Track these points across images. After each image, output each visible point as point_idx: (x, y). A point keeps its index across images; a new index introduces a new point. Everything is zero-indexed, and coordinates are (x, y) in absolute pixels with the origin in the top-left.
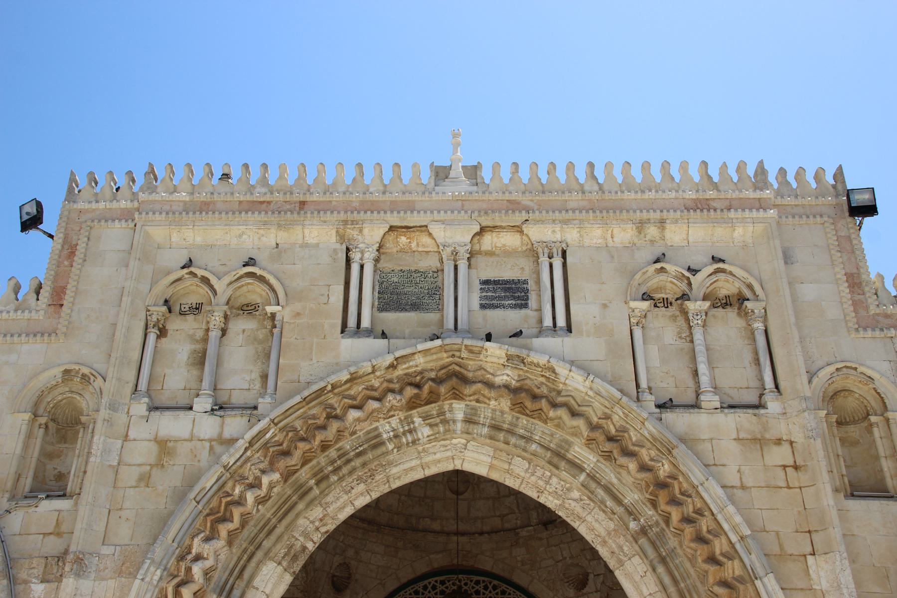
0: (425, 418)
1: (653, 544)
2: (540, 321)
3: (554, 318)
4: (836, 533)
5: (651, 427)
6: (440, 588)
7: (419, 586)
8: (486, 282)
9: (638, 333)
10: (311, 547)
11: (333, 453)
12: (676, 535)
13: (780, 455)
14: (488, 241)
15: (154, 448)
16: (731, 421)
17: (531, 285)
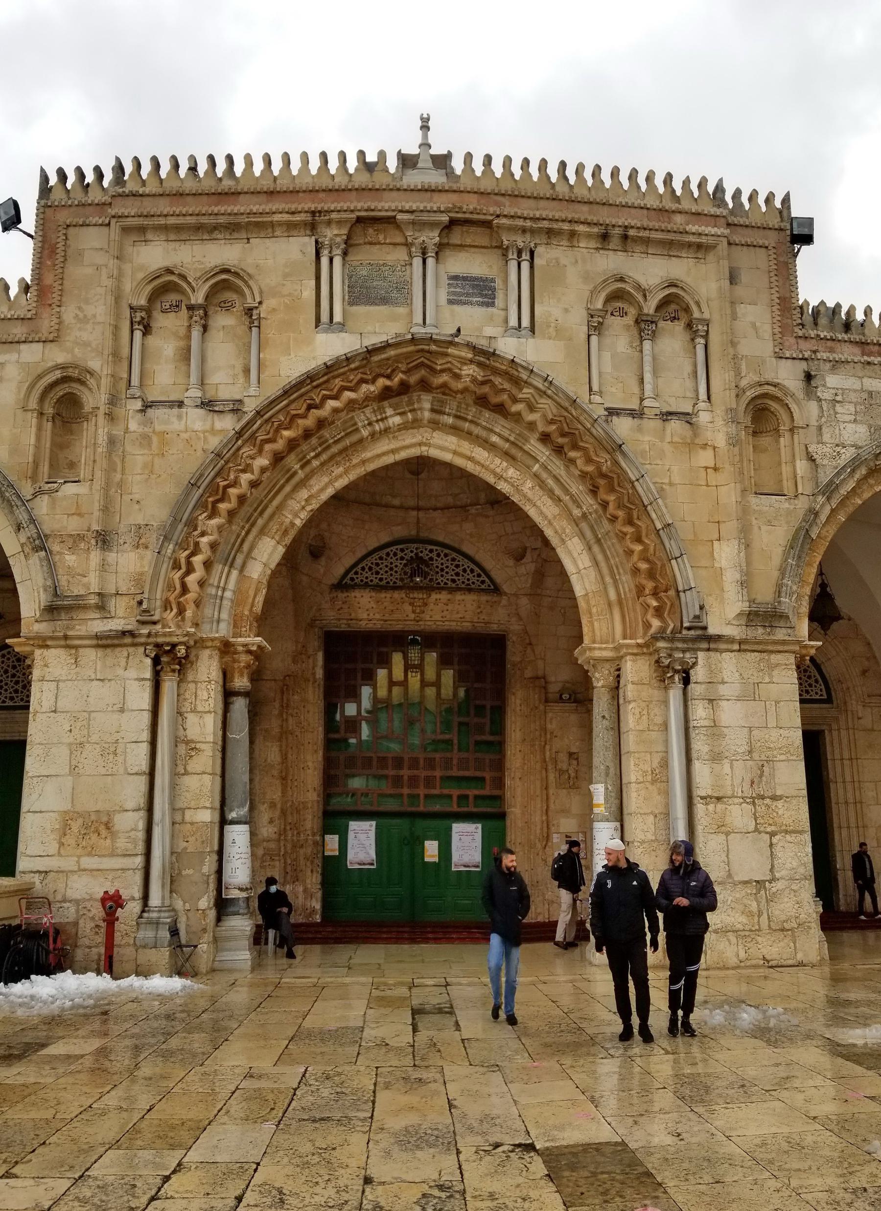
1: (592, 528)
3: (519, 319)
6: (400, 554)
7: (383, 553)
10: (298, 523)
12: (610, 520)
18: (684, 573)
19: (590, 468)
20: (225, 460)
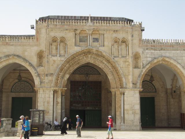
2: (100, 44)
5: (113, 60)
7: (81, 68)
8: (93, 38)
9: (112, 46)
10: (71, 72)
11: (74, 61)
14: (94, 32)
15: (53, 61)
16: (123, 59)
18: (124, 80)
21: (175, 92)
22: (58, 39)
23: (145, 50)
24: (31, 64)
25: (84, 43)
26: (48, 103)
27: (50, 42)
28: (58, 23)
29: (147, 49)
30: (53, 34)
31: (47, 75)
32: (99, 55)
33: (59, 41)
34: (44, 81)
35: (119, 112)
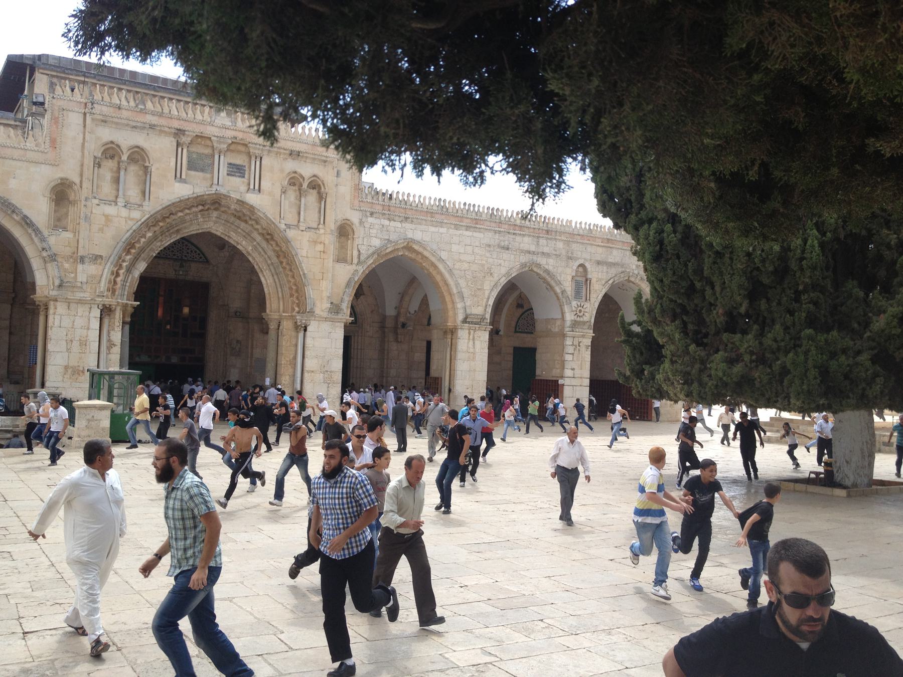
0: (202, 215)
2: (249, 184)
4: (330, 275)
8: (230, 164)
13: (320, 247)
14: (232, 147)
15: (104, 218)
16: (308, 235)
17: (247, 169)
19: (277, 249)
20: (138, 233)
21: (404, 325)
22: (125, 151)
23: (367, 216)
24: (31, 221)
25: (200, 174)
26: (84, 343)
27: (95, 157)
28: (124, 103)
29: (372, 214)
30: (106, 134)
31: (82, 260)
32: (245, 214)
33: (124, 158)
34: (73, 275)
35: (287, 377)
